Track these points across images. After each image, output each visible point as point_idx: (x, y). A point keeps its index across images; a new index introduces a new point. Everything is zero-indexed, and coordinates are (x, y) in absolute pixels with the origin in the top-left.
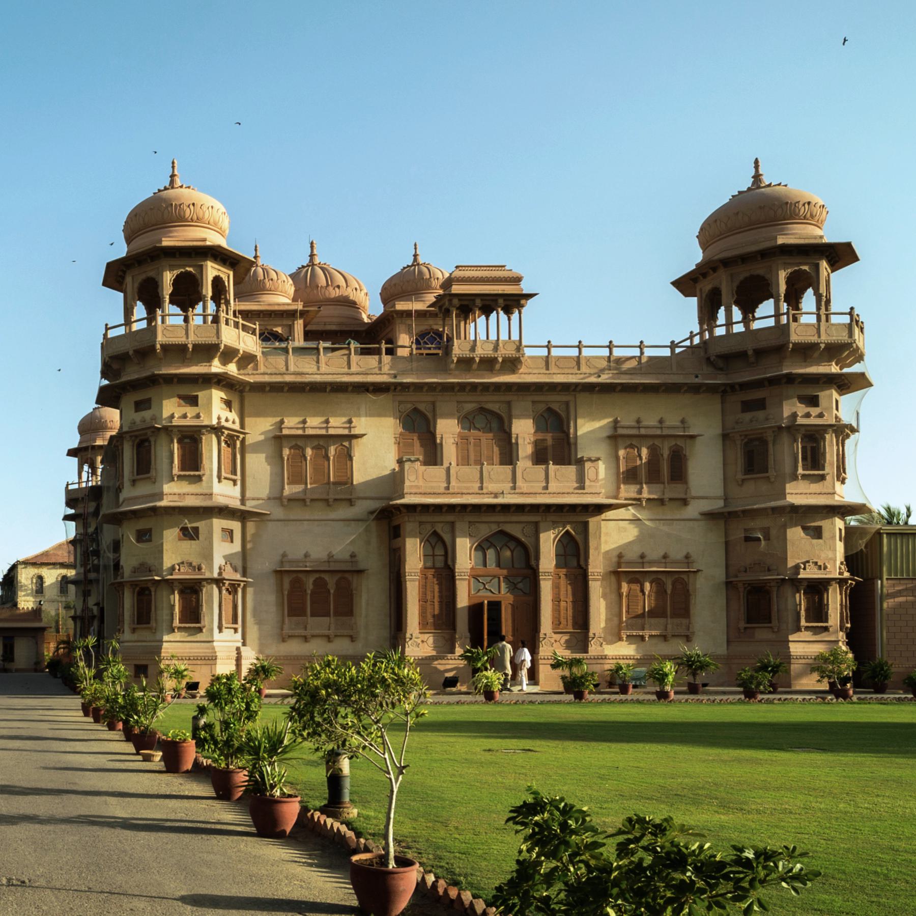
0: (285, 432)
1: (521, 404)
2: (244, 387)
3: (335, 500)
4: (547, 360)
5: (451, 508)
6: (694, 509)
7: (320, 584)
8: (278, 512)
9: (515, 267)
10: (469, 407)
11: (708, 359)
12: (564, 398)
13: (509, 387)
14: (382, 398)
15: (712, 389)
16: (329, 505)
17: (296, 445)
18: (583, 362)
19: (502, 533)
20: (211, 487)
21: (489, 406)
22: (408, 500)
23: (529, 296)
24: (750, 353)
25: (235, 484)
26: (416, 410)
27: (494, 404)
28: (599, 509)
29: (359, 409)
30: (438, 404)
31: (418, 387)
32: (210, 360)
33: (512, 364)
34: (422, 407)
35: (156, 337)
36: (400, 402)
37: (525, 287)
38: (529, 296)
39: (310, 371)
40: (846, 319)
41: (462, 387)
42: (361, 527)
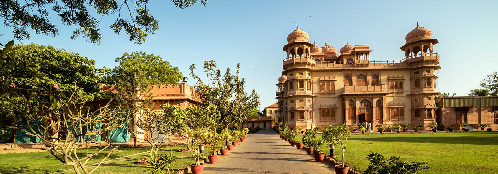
1: (369, 73)
5: (355, 95)
6: (404, 94)
7: (328, 110)
8: (319, 96)
9: (368, 45)
13: (367, 70)
15: (408, 70)
19: (365, 100)
22: (346, 93)
28: (385, 94)
31: (348, 70)
33: (367, 65)
37: (370, 49)
41: (357, 70)
42: (337, 99)
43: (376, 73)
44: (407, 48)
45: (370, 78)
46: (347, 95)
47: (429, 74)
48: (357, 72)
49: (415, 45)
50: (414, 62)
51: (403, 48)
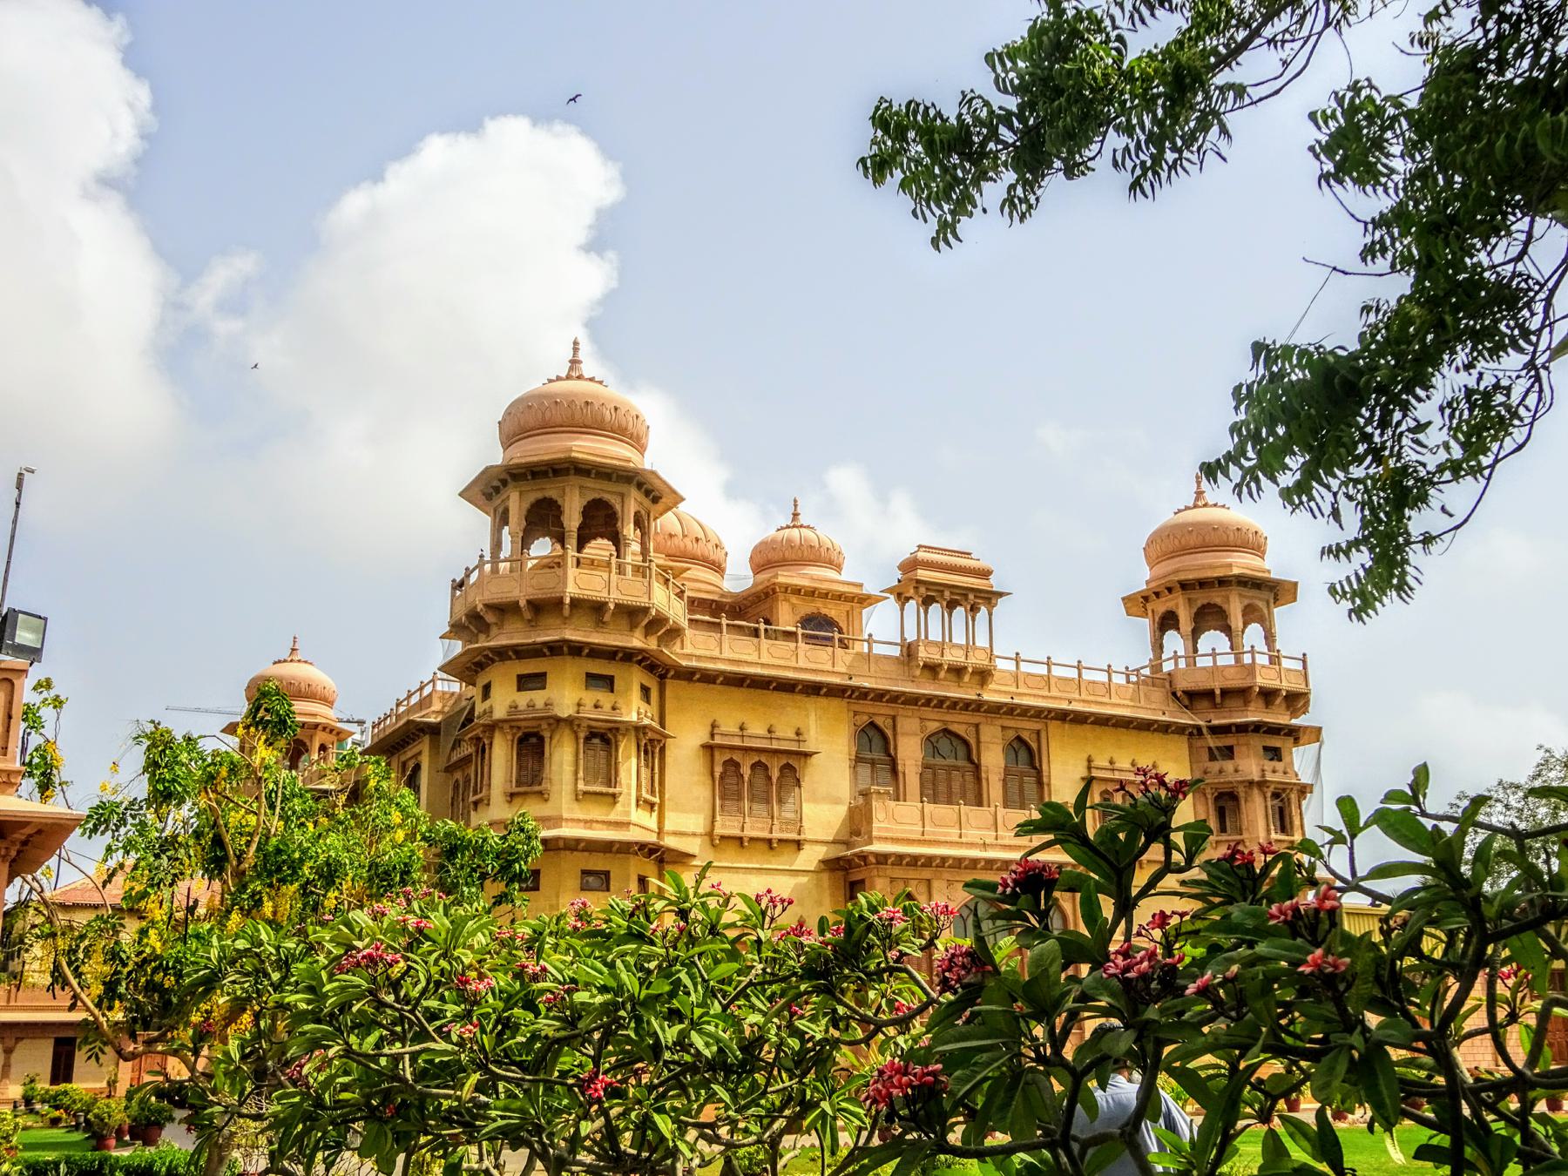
0: (718, 740)
2: (668, 671)
3: (780, 840)
4: (1047, 679)
5: (929, 861)
10: (933, 726)
11: (1174, 694)
12: (1035, 726)
14: (836, 704)
15: (1181, 730)
16: (771, 848)
17: (731, 760)
18: (1052, 682)
20: (628, 813)
21: (954, 728)
22: (877, 847)
23: (1001, 595)
24: (1218, 692)
25: (652, 809)
26: (872, 724)
27: (960, 724)
29: (807, 716)
30: (900, 721)
31: (880, 696)
32: (633, 627)
33: (983, 675)
34: (879, 721)
35: (565, 584)
36: (856, 713)
37: (995, 583)
38: (1001, 595)
39: (749, 659)
40: (1298, 666)
41: (929, 701)
43: (1027, 727)
44: (1161, 607)
45: (993, 759)
46: (882, 858)
47: (1279, 766)
48: (928, 712)
49: (1201, 598)
50: (1209, 694)
51: (1137, 603)
